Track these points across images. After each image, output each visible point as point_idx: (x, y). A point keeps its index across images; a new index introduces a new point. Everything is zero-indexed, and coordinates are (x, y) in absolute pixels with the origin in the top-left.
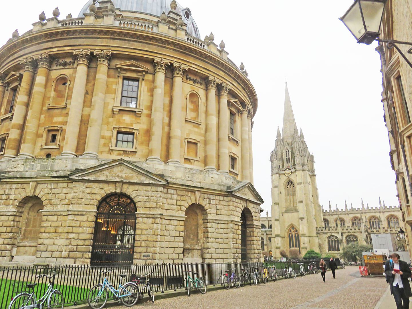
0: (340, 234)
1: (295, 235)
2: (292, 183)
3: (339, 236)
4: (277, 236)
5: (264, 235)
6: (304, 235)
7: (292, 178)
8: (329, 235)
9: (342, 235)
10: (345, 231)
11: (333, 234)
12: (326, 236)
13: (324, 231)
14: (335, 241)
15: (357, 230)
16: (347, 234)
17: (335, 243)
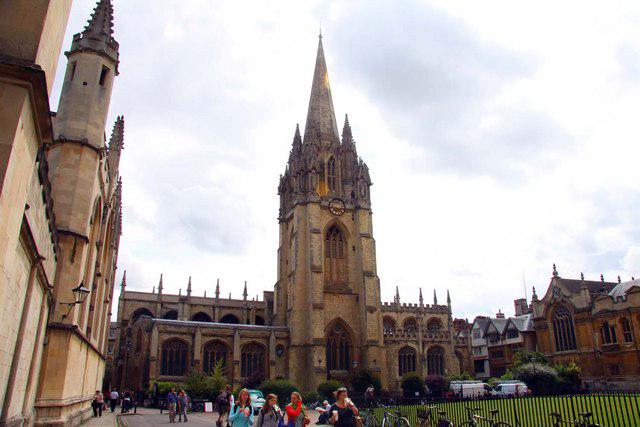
0: (421, 343)
1: (341, 344)
2: (338, 231)
3: (419, 349)
4: (317, 342)
5: (268, 338)
6: (374, 343)
7: (346, 219)
8: (402, 345)
9: (423, 346)
10: (428, 339)
11: (410, 344)
12: (398, 347)
13: (394, 338)
14: (409, 357)
15: (444, 339)
16: (430, 345)
17: (409, 361)
